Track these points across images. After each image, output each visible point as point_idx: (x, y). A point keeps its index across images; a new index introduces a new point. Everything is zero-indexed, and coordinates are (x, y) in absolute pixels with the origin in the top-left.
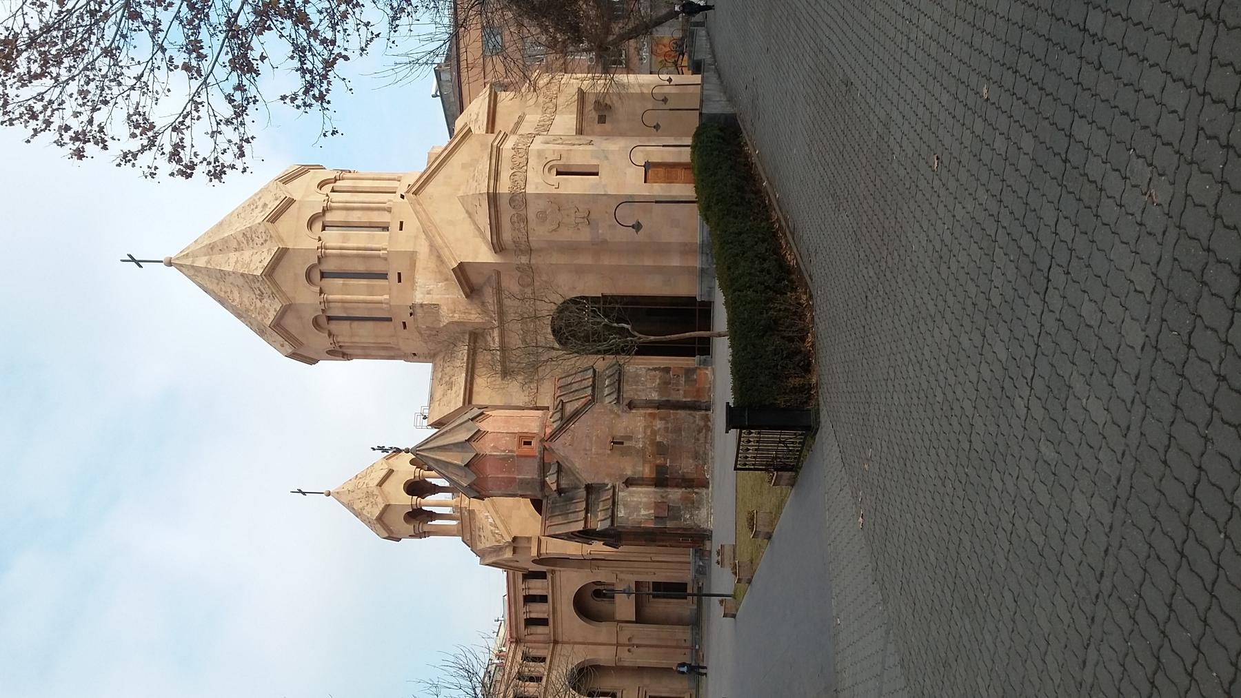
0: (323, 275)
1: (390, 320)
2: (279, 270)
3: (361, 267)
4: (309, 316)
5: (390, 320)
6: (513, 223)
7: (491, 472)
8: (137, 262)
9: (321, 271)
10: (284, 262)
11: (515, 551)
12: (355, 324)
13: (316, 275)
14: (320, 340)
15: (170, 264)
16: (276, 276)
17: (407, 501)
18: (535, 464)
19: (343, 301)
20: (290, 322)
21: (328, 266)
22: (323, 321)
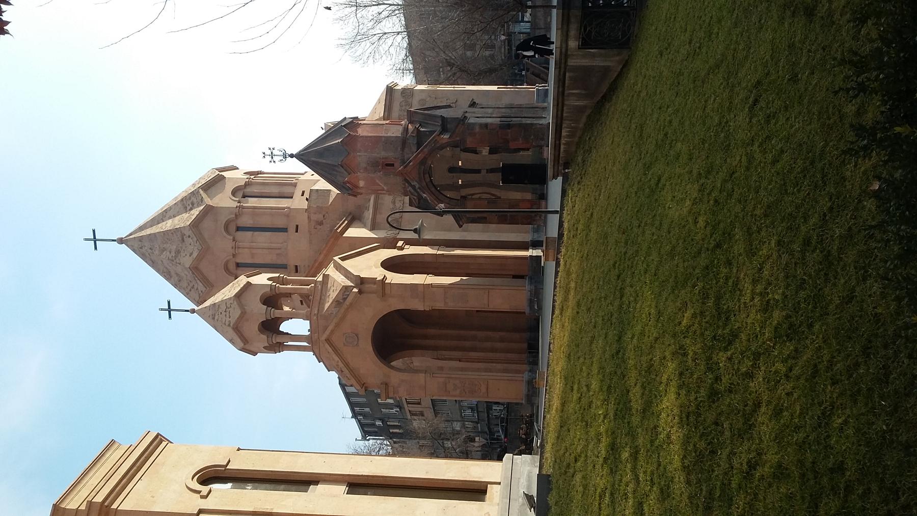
0: (244, 197)
1: (284, 230)
2: (213, 188)
3: (275, 190)
4: (223, 219)
5: (284, 230)
6: (401, 106)
7: (361, 132)
8: (95, 240)
9: (242, 192)
10: (219, 185)
11: (360, 292)
12: (256, 233)
13: (240, 194)
14: (223, 245)
15: (121, 241)
16: (209, 191)
17: (270, 283)
18: (401, 129)
19: (255, 208)
20: (207, 224)
21: (249, 190)
22: (232, 228)
